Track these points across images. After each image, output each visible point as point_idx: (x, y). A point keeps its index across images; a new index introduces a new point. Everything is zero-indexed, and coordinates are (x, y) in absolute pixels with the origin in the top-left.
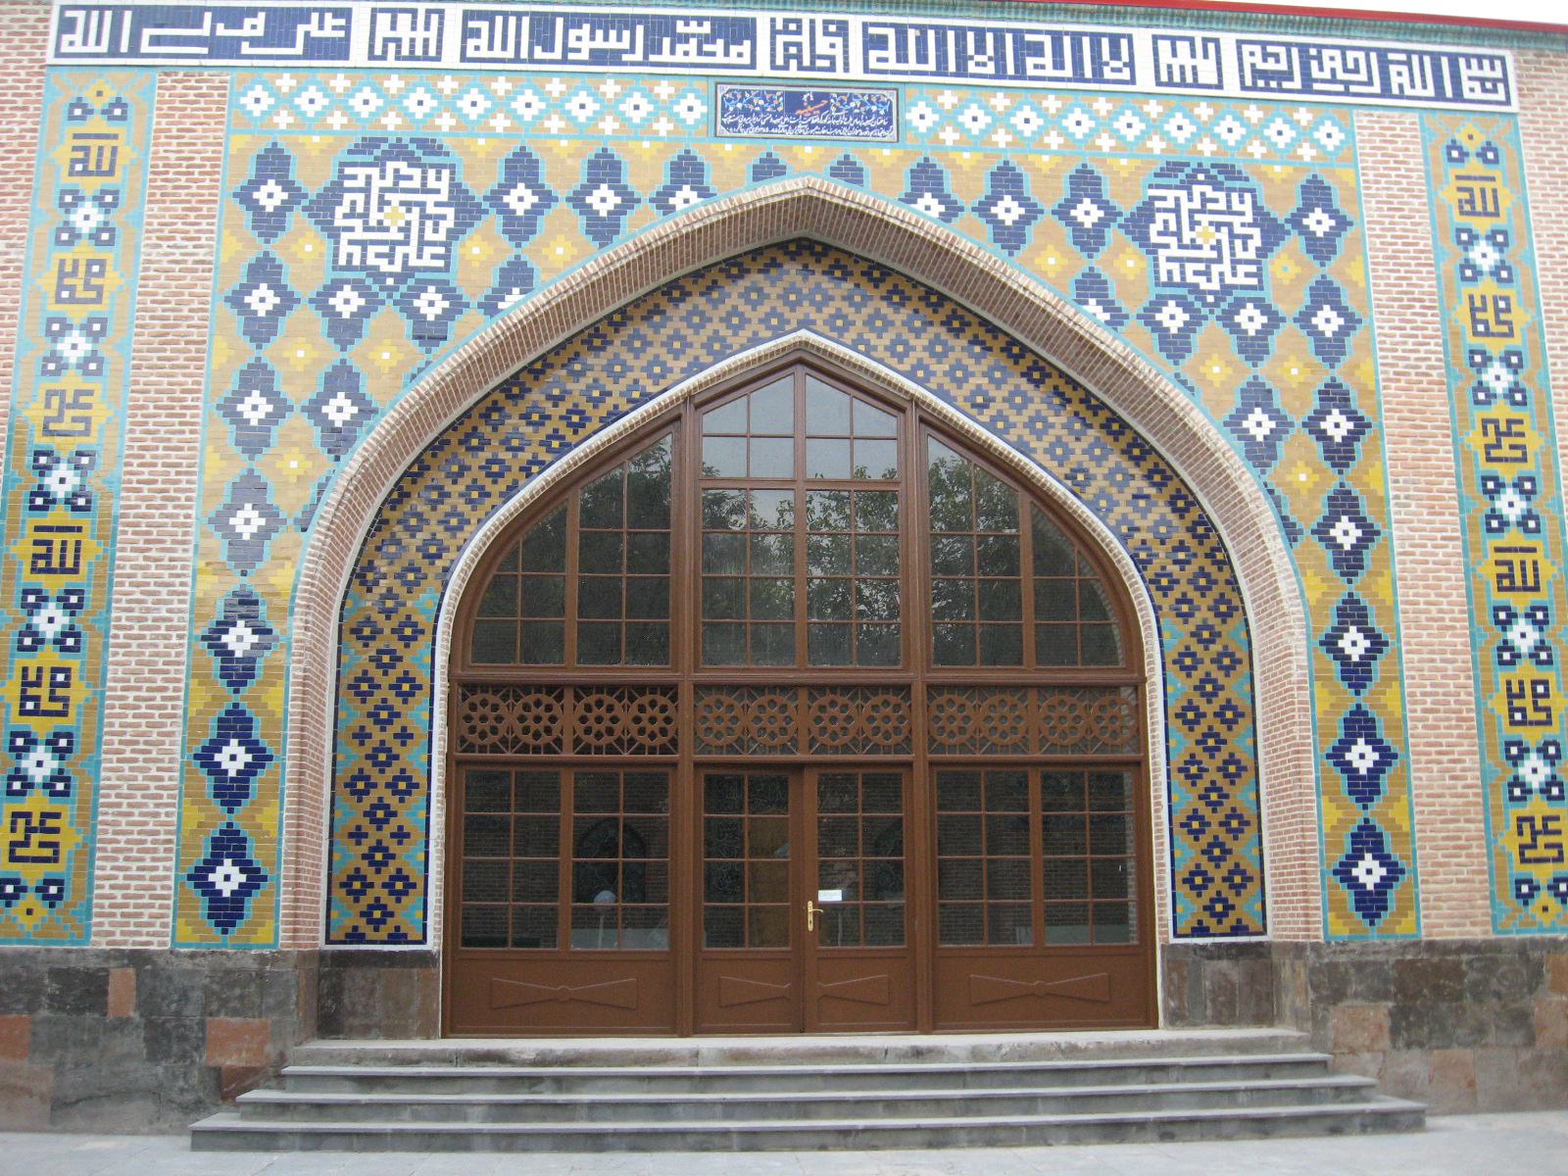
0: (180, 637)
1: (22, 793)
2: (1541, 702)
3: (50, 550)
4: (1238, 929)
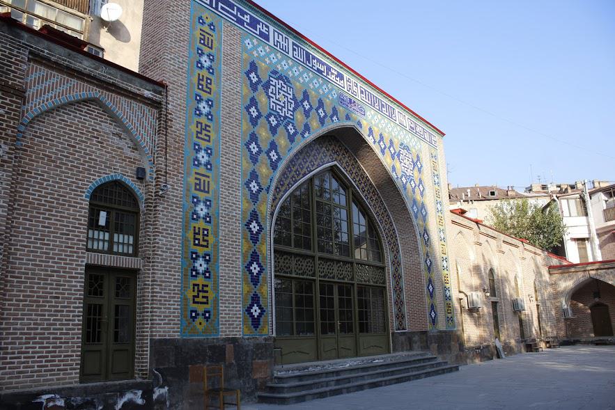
0: (239, 223)
1: (195, 276)
3: (200, 182)
4: (403, 329)
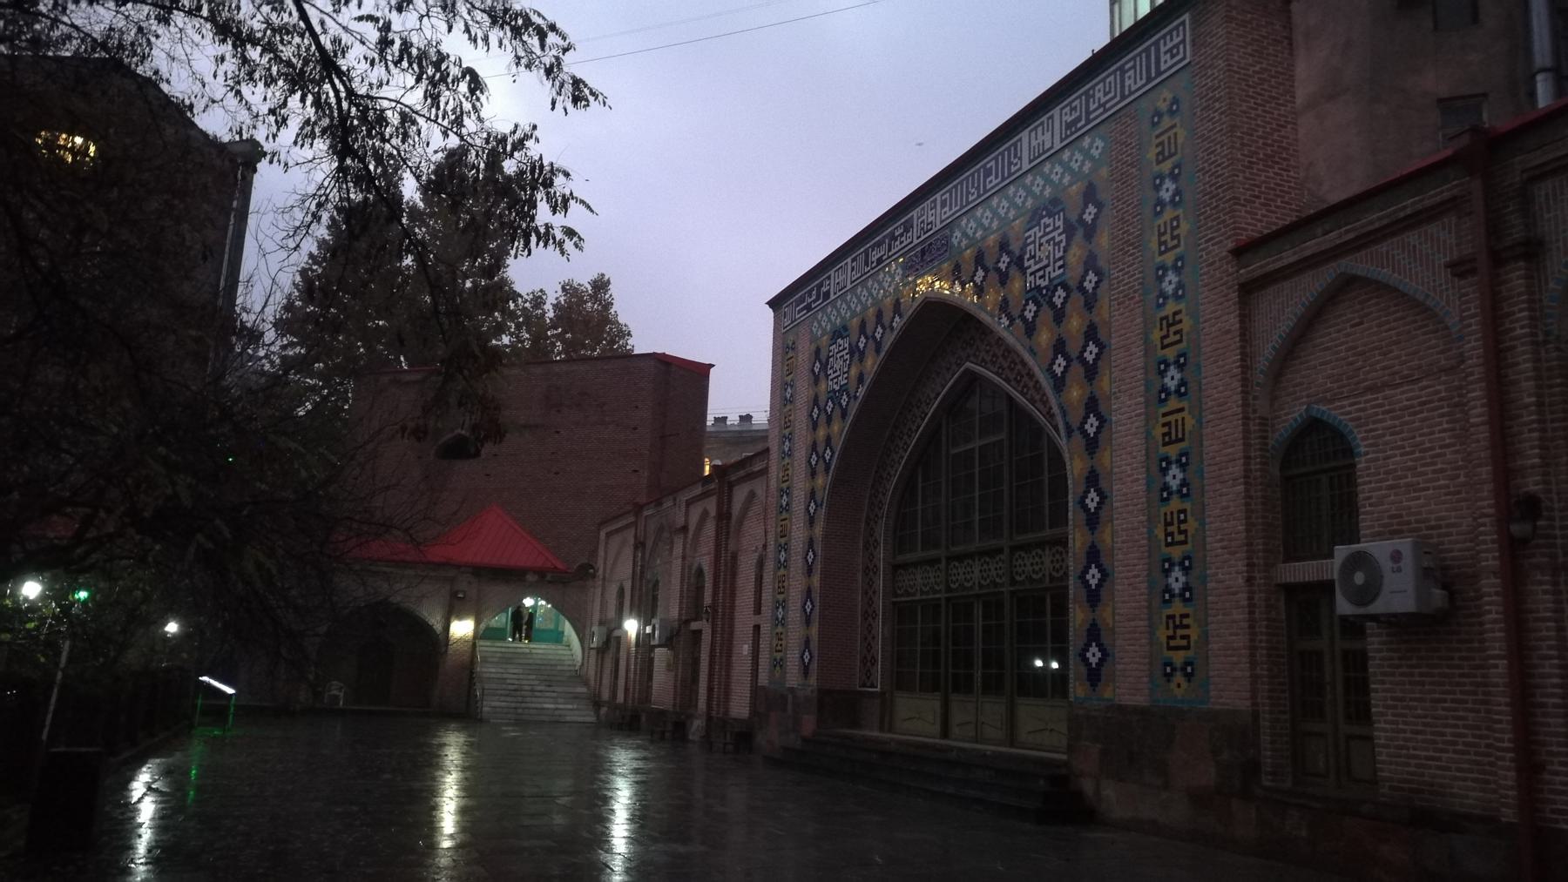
2: (1183, 527)
